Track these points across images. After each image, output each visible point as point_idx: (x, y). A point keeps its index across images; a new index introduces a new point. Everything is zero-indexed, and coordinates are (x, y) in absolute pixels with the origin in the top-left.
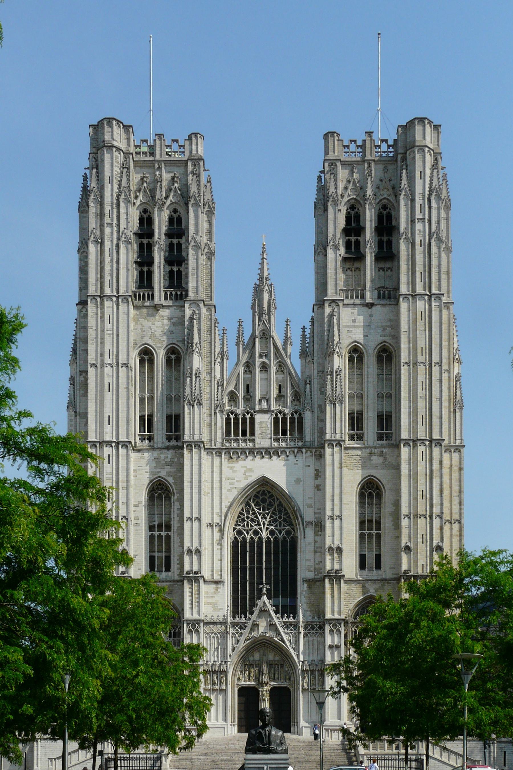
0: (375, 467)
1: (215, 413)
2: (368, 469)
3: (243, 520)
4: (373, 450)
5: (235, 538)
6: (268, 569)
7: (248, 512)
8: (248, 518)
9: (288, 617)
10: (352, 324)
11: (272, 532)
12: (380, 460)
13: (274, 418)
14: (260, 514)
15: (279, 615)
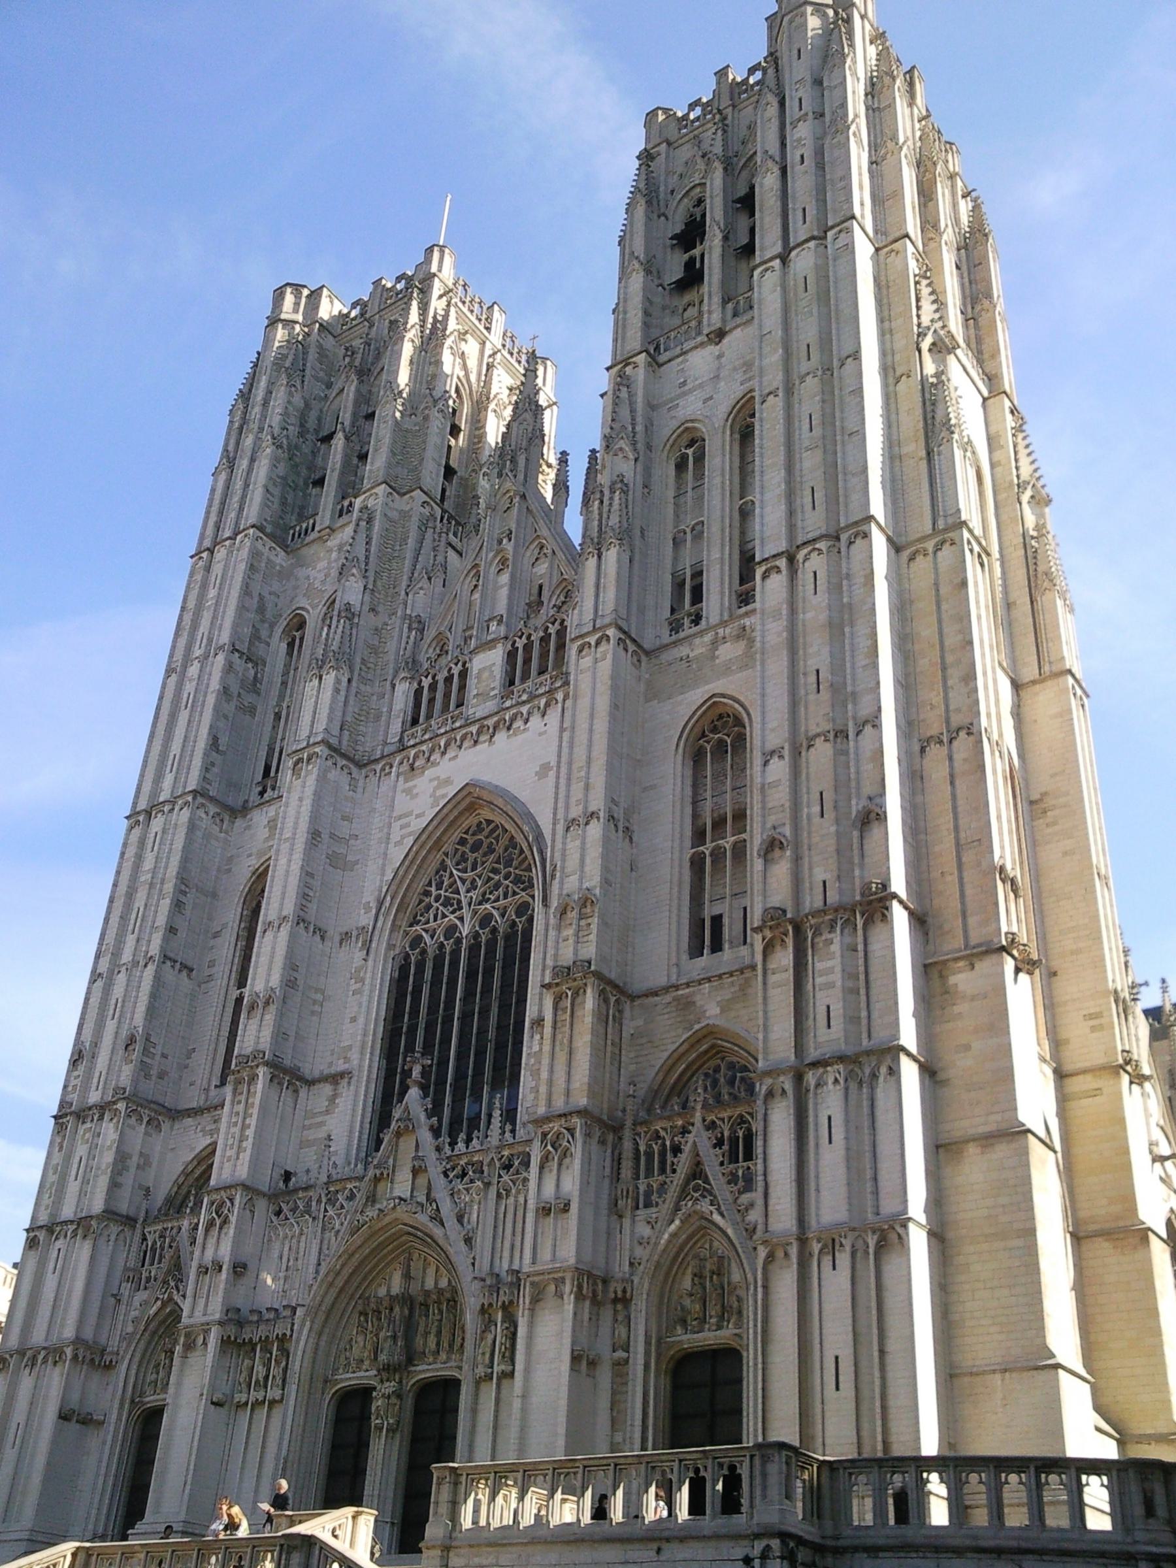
0: (727, 670)
1: (393, 686)
2: (707, 683)
3: (429, 907)
4: (721, 631)
5: (407, 957)
6: (466, 1017)
7: (439, 887)
8: (437, 899)
9: (468, 1141)
10: (679, 391)
11: (486, 920)
12: (741, 646)
13: (509, 653)
14: (463, 881)
15: (445, 1139)
